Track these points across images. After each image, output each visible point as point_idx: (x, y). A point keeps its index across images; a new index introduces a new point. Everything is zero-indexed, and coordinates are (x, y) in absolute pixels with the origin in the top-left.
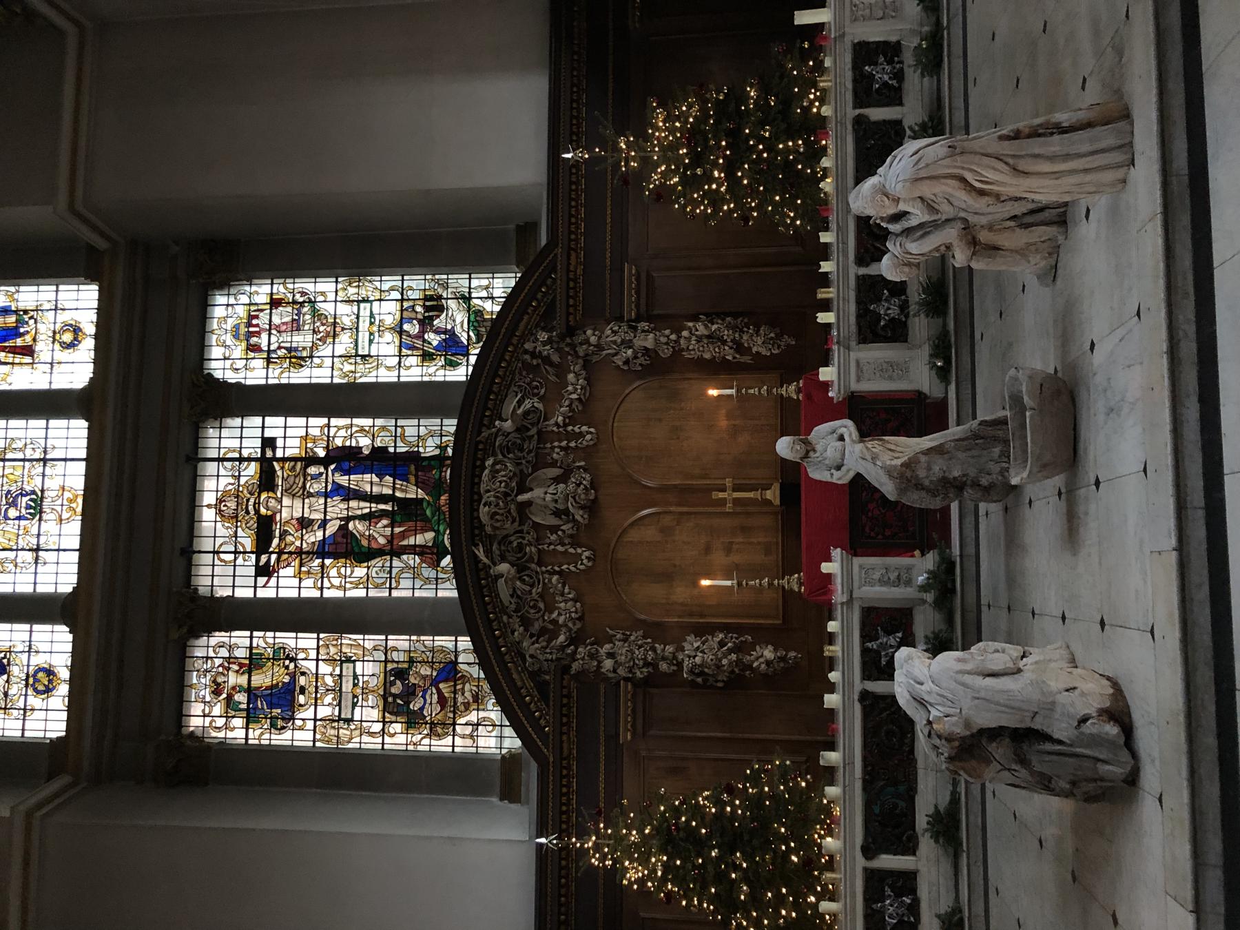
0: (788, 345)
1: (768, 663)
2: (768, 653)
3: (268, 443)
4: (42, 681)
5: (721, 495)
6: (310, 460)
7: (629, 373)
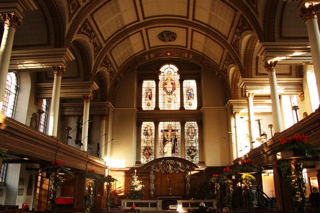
3: (177, 131)
4: (149, 105)
6: (175, 136)
7: (184, 177)
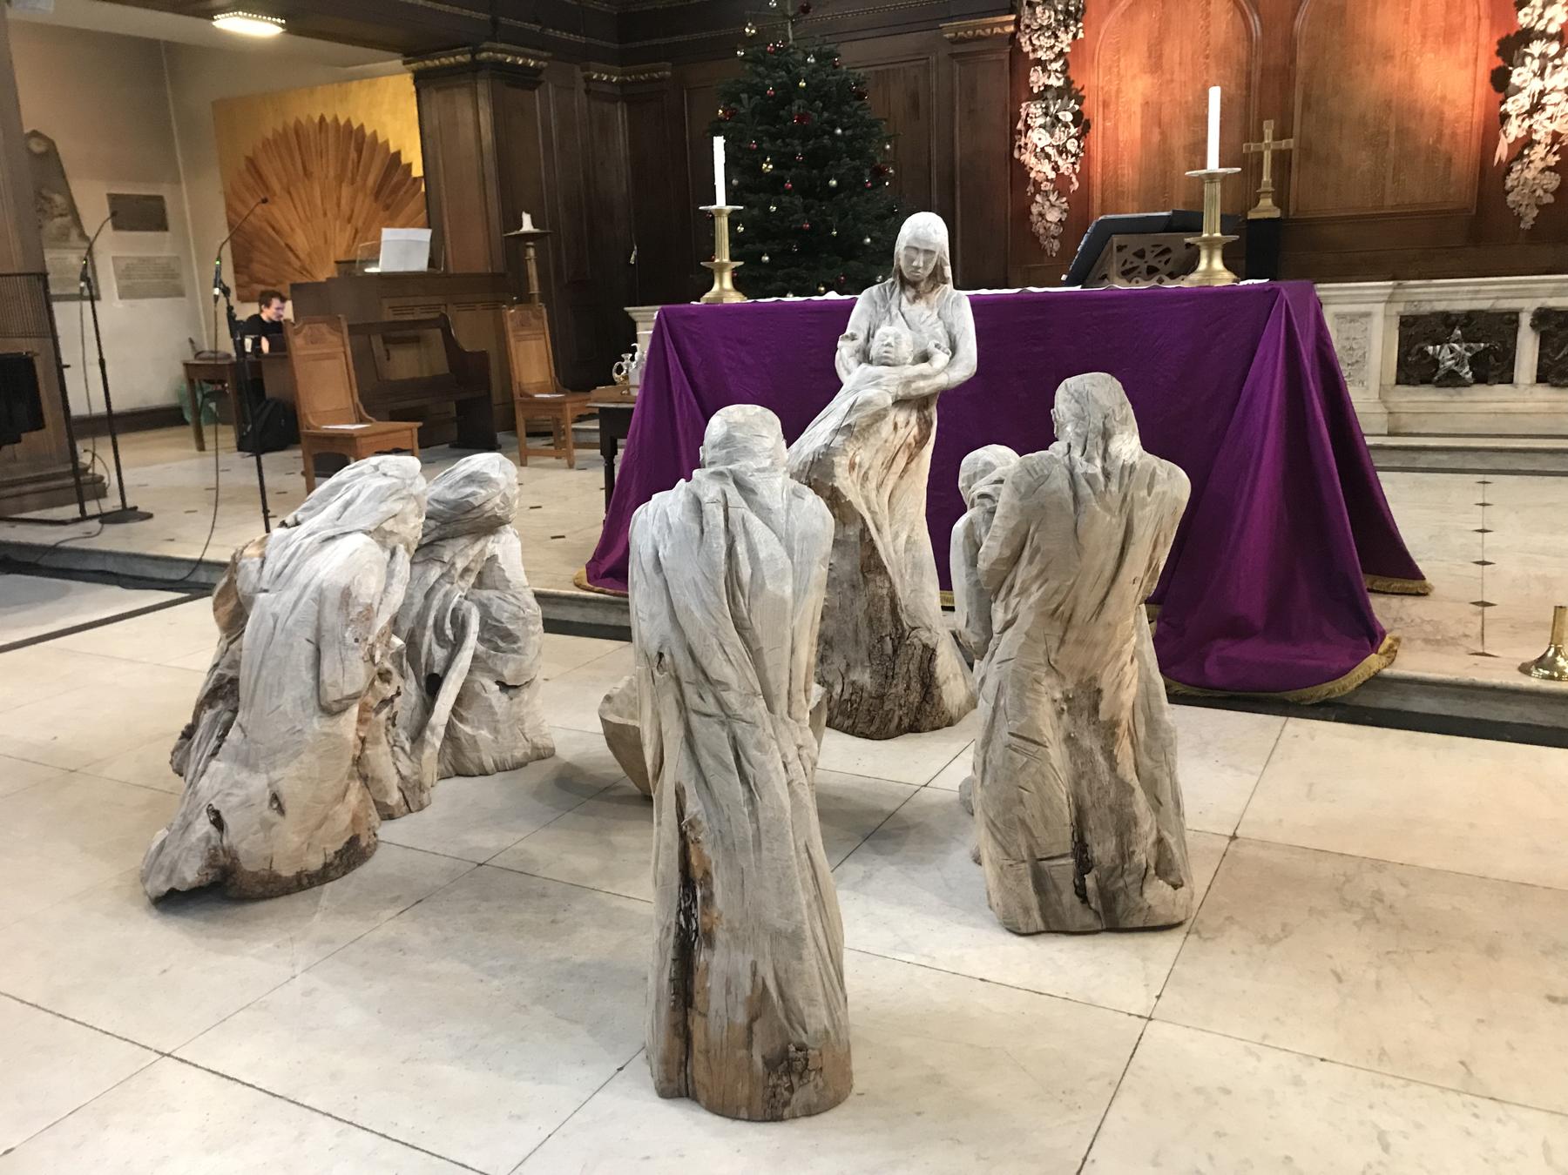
0: (1519, 218)
1: (1042, 215)
2: (1053, 216)
5: (1268, 132)
